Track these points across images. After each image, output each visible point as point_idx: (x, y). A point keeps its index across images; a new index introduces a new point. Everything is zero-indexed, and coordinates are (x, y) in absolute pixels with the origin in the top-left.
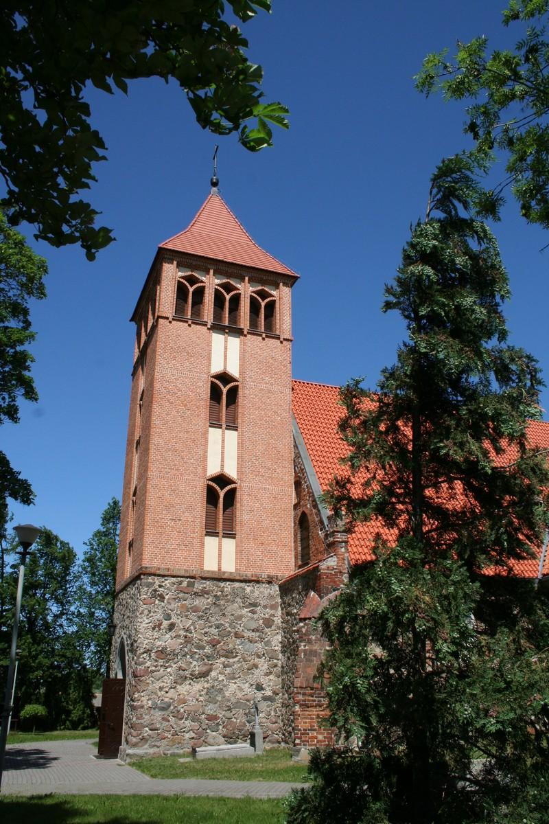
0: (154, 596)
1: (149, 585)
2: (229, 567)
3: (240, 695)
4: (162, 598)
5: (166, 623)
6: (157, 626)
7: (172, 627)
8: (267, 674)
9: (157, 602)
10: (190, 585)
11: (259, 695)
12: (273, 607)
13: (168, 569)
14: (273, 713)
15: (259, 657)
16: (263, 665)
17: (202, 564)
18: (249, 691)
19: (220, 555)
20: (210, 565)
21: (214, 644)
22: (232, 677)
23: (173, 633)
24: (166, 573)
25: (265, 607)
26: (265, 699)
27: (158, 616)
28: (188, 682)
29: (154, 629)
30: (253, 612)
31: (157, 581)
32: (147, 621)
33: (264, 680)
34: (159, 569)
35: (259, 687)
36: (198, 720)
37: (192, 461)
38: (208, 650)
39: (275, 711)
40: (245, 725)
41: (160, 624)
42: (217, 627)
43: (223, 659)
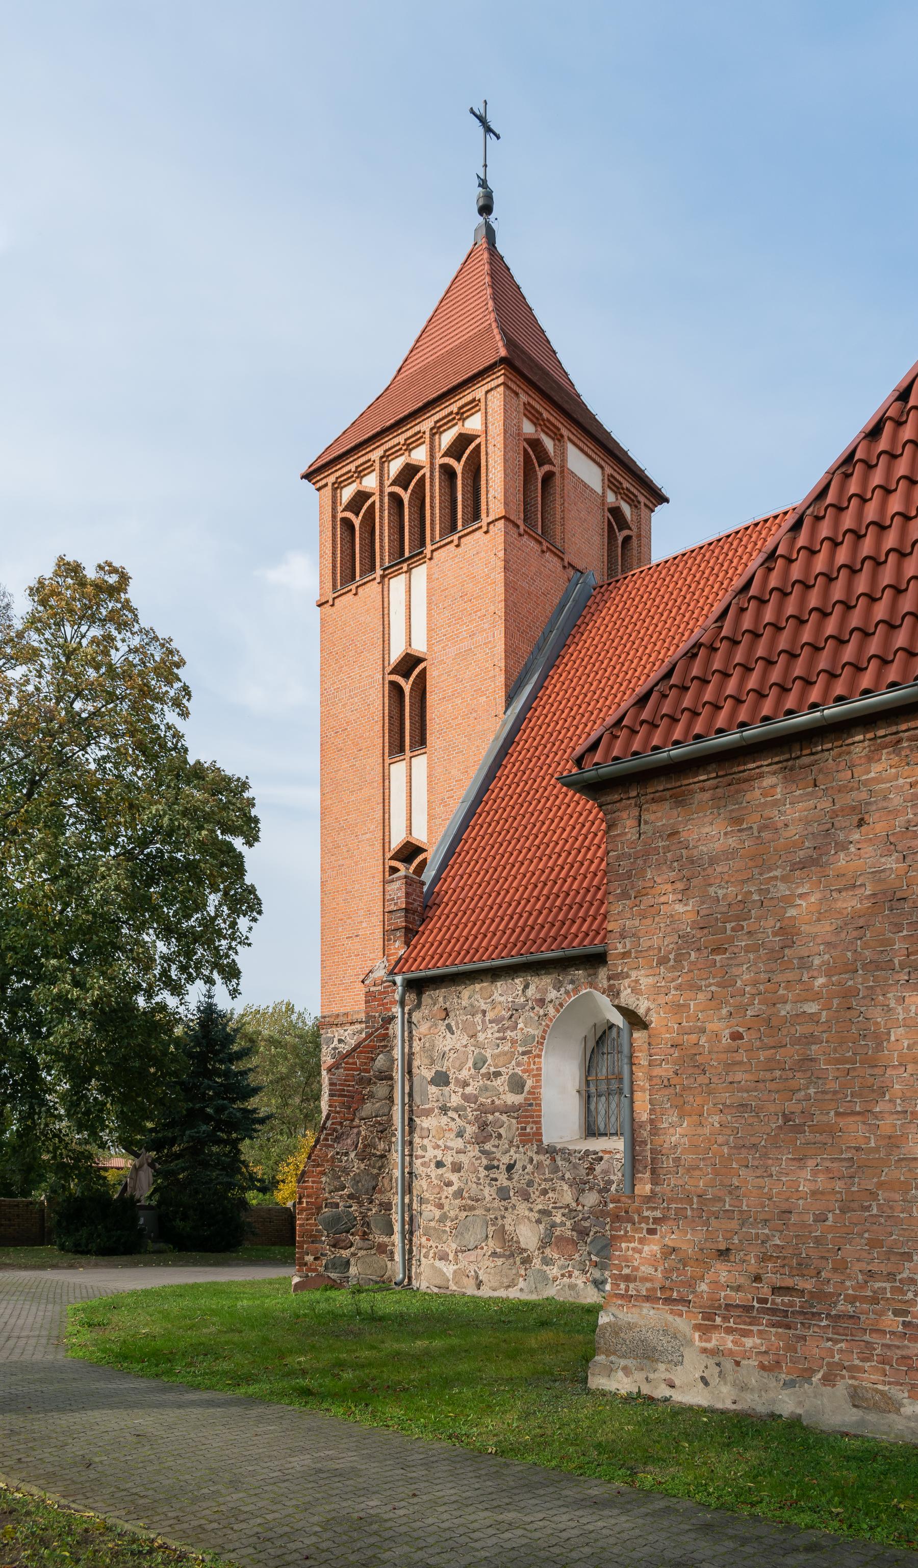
13: (346, 1014)
24: (344, 1020)
34: (338, 1015)
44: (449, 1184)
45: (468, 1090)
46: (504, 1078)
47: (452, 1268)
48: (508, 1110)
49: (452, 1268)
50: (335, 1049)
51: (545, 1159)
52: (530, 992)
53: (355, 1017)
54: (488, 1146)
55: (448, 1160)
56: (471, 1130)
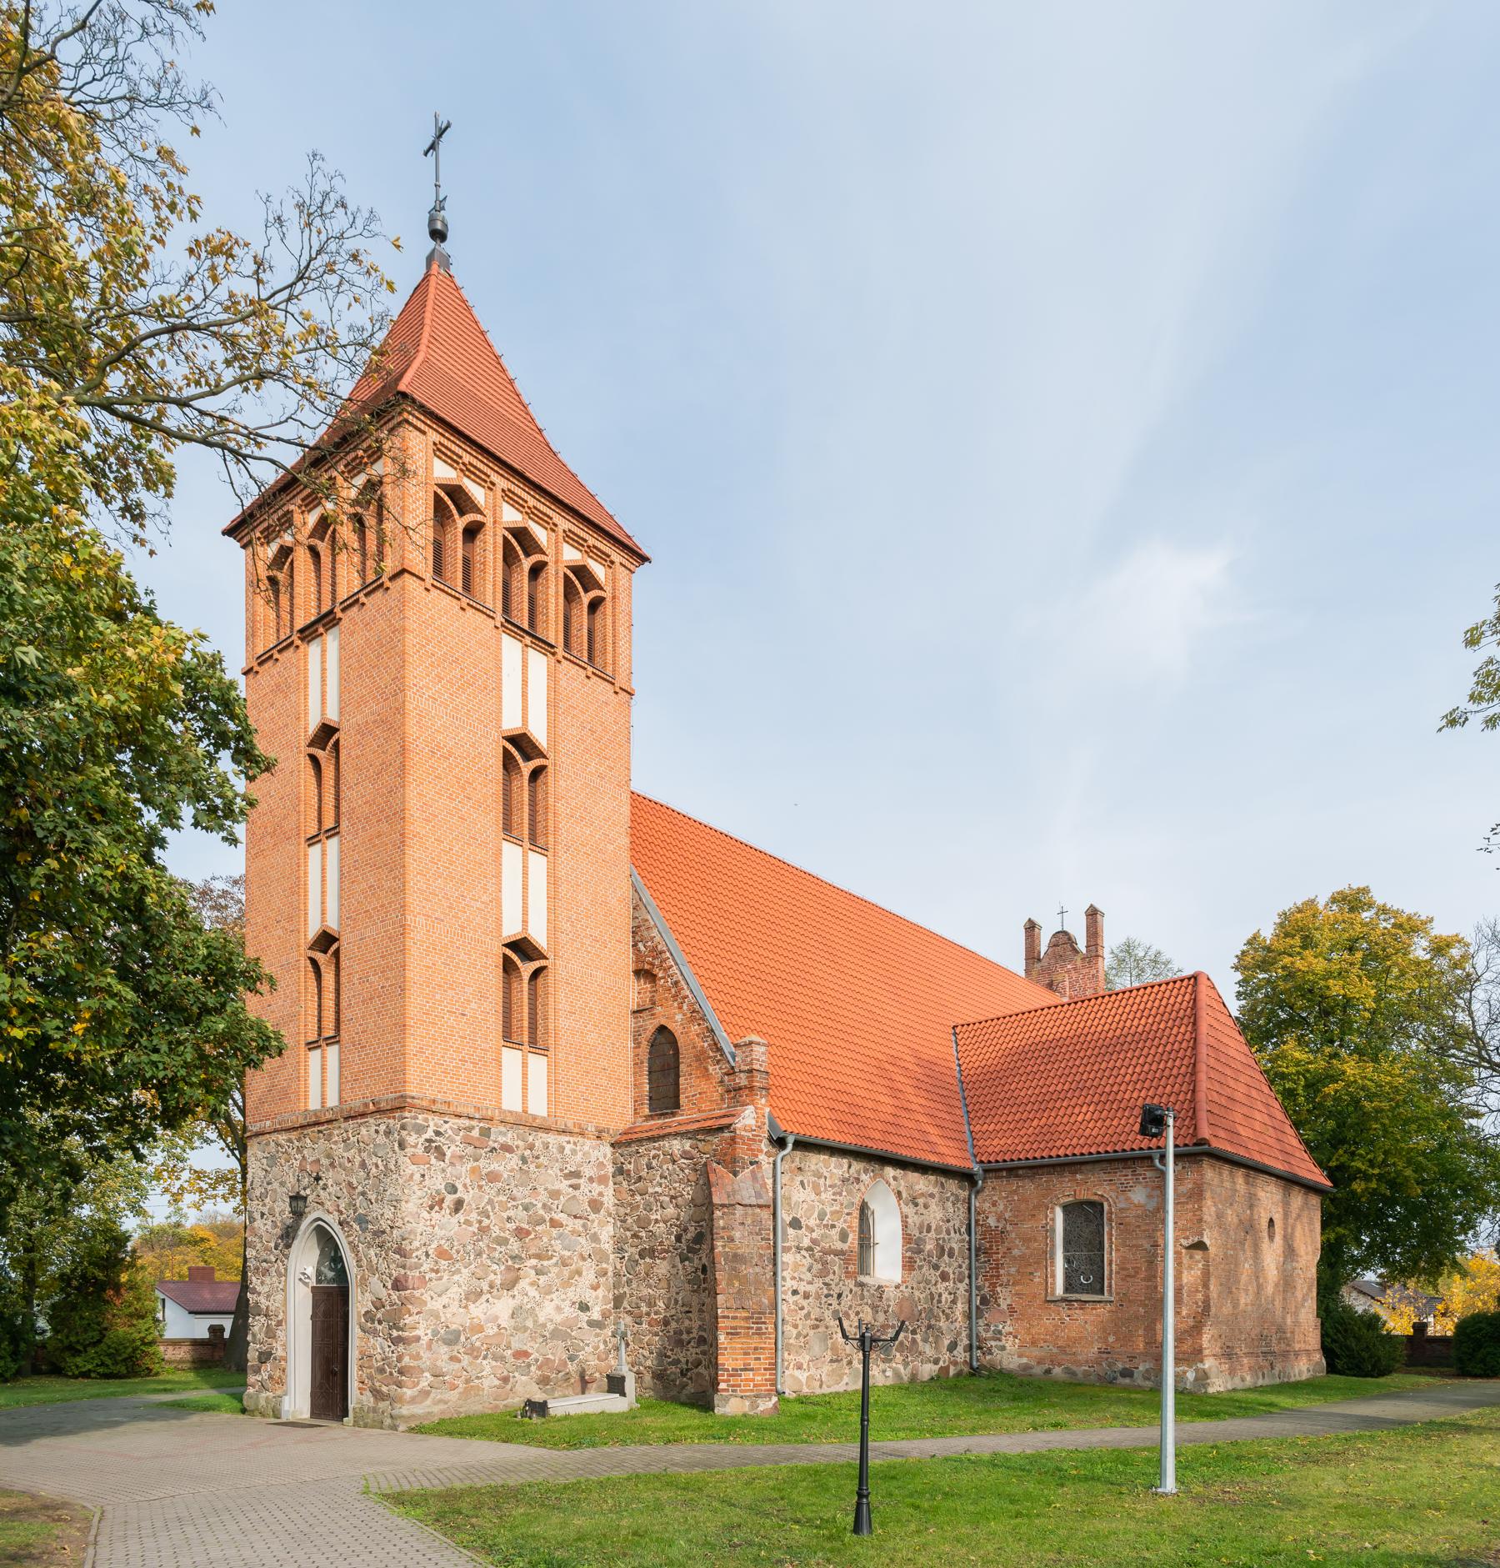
0: (427, 1149)
1: (420, 1130)
2: (539, 1107)
3: (558, 1318)
4: (441, 1155)
5: (450, 1199)
6: (436, 1203)
7: (458, 1205)
8: (595, 1288)
9: (433, 1161)
10: (485, 1133)
11: (584, 1317)
12: (602, 1180)
14: (602, 1347)
15: (584, 1259)
16: (589, 1276)
17: (499, 1100)
18: (570, 1312)
19: (523, 1082)
20: (511, 1101)
21: (520, 1233)
22: (548, 1291)
23: (461, 1216)
24: (444, 1108)
25: (591, 1180)
26: (591, 1323)
27: (438, 1183)
28: (484, 1297)
29: (432, 1207)
30: (575, 1187)
31: (434, 1122)
32: (419, 1193)
33: (589, 1296)
34: (434, 1101)
35: (584, 1307)
36: (502, 1358)
37: (479, 904)
38: (514, 1246)
39: (605, 1342)
40: (565, 1364)
41: (442, 1200)
42: (526, 1209)
43: (534, 1262)
44: (802, 1308)
45: (814, 1235)
46: (838, 1230)
47: (806, 1374)
48: (837, 1253)
49: (806, 1374)
50: (429, 1141)
51: (858, 1289)
52: (852, 1170)
53: (459, 1110)
54: (827, 1280)
55: (801, 1289)
56: (817, 1267)
